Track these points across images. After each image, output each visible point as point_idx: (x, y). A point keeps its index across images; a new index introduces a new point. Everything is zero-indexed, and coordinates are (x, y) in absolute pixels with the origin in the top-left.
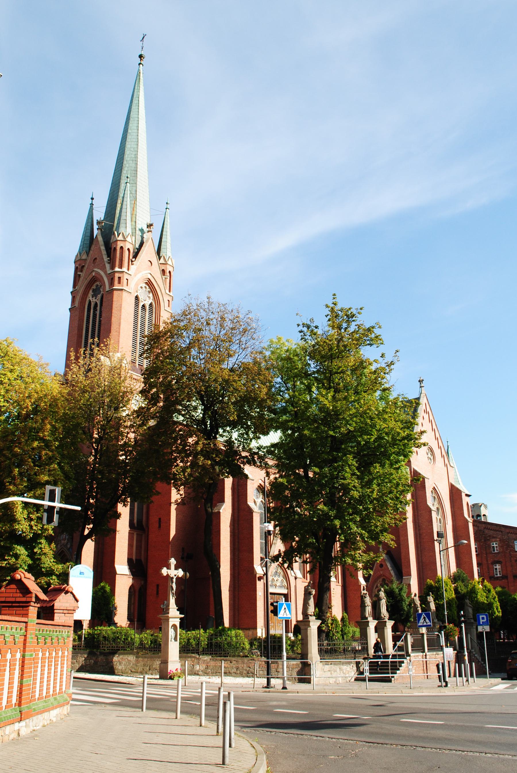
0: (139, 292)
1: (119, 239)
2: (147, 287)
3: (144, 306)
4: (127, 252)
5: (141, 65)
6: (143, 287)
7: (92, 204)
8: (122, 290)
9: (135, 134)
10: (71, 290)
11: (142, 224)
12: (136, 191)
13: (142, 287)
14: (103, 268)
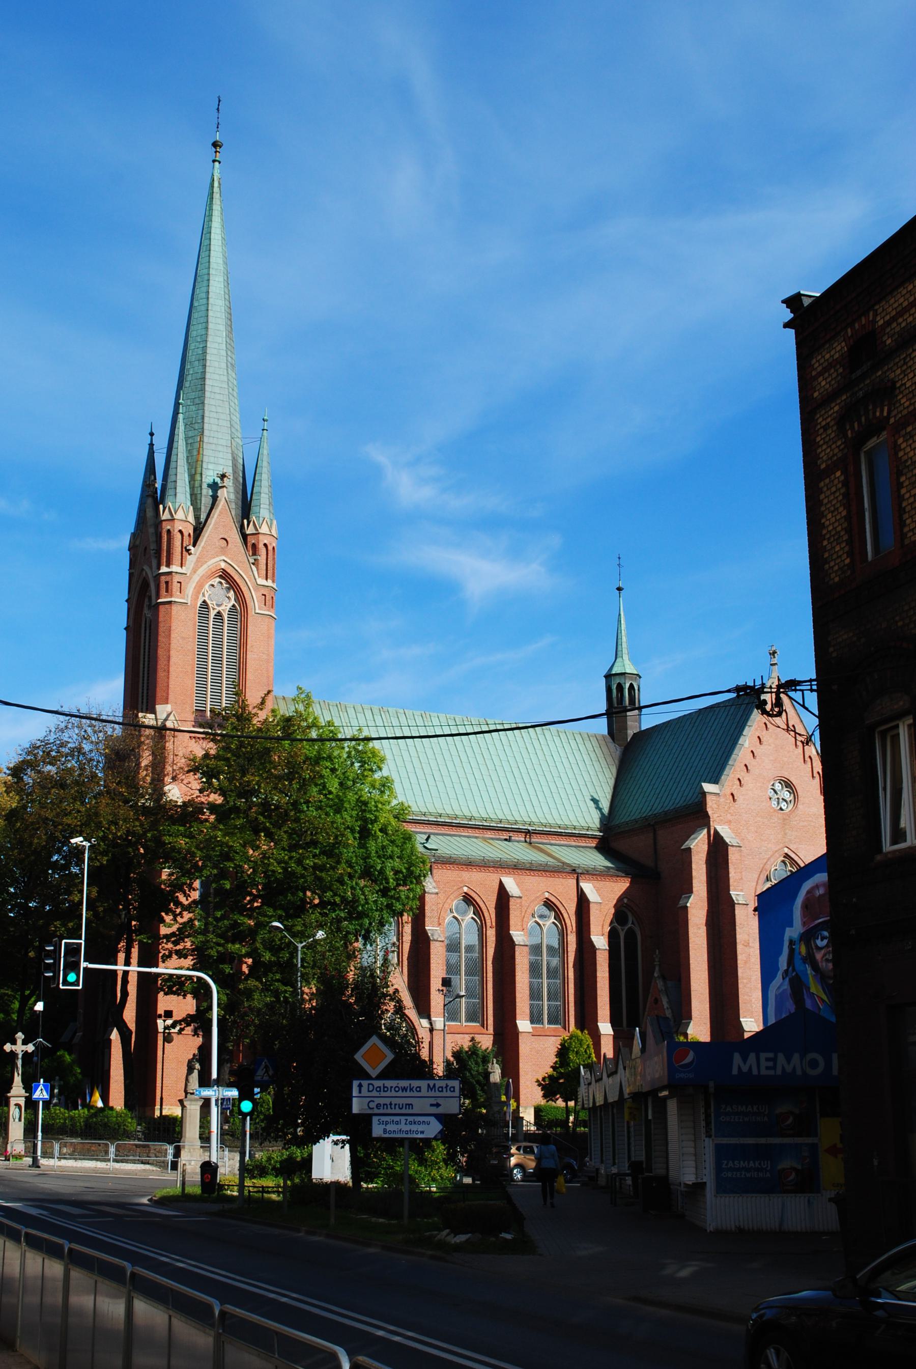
0: (207, 595)
1: (163, 518)
2: (223, 581)
3: (219, 614)
4: (179, 536)
5: (217, 164)
6: (215, 584)
7: (151, 445)
8: (170, 603)
9: (203, 308)
10: (126, 597)
11: (210, 475)
12: (203, 417)
13: (213, 586)
14: (151, 567)
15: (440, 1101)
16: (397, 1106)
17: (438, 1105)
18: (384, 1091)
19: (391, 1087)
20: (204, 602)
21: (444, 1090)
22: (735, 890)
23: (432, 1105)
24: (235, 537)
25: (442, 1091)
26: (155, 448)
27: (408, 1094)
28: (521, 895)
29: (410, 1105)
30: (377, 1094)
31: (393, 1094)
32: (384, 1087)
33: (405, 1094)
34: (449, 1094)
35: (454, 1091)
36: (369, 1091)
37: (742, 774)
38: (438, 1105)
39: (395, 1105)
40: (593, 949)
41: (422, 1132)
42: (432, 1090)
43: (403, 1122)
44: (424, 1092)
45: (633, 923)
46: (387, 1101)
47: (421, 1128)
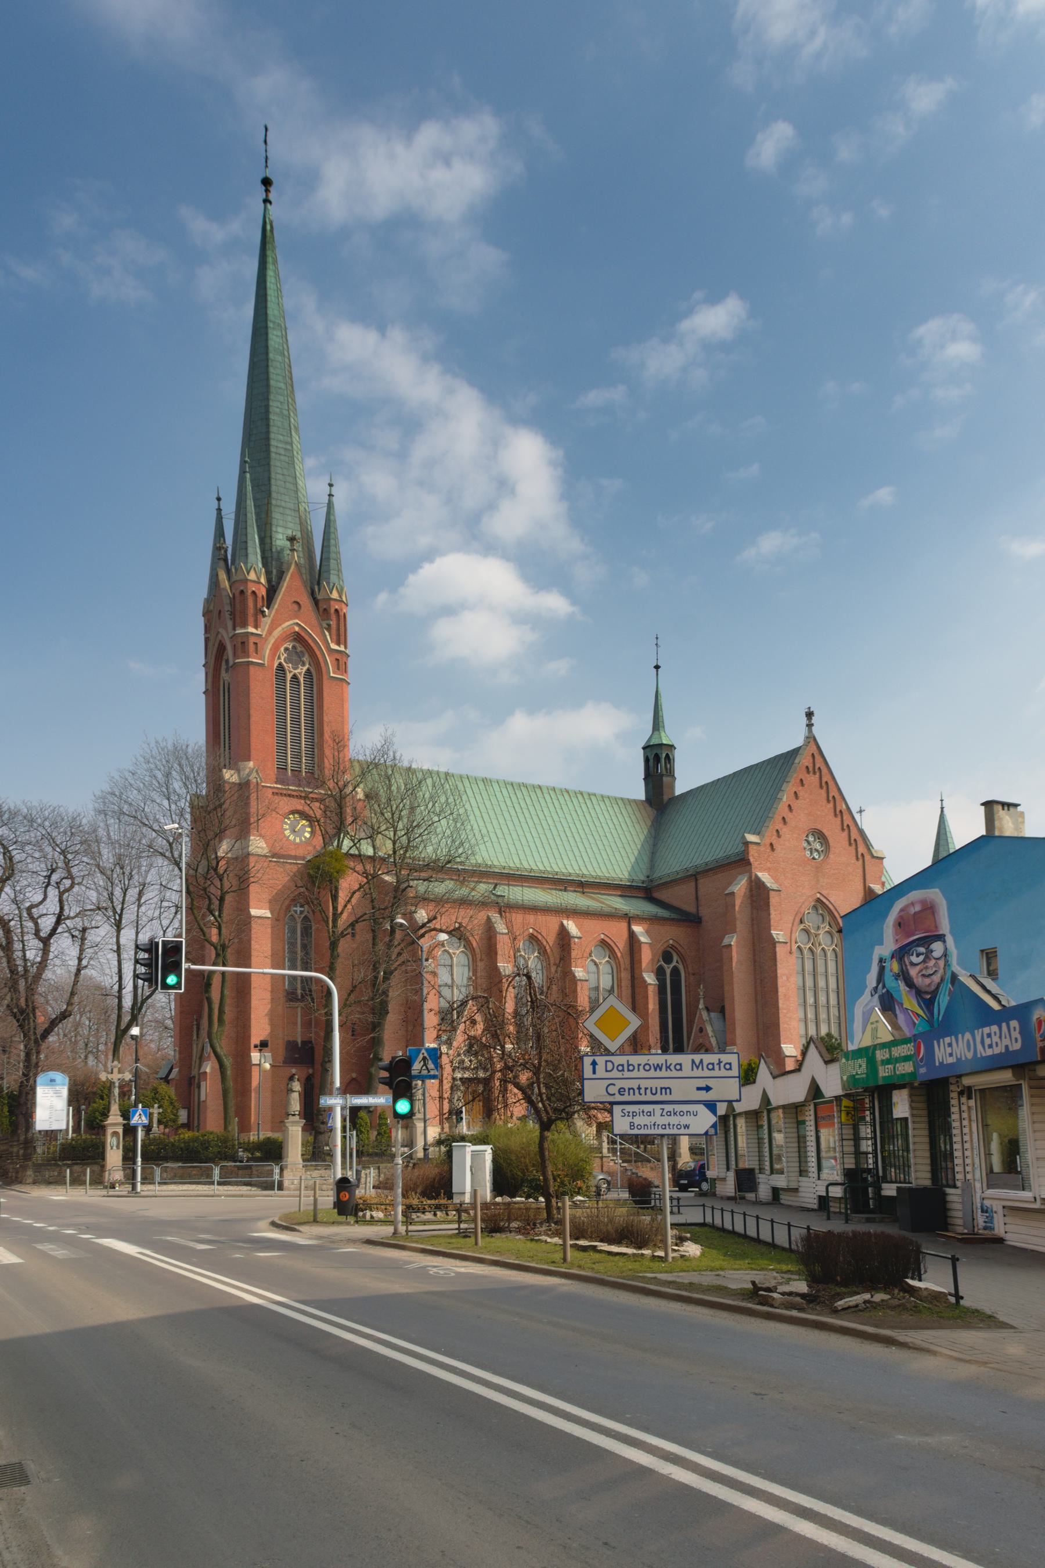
7: (219, 510)
14: (226, 629)
15: (710, 1083)
16: (648, 1091)
17: (708, 1089)
18: (629, 1070)
19: (639, 1065)
20: (280, 664)
21: (716, 1067)
23: (699, 1089)
24: (306, 601)
25: (713, 1069)
26: (223, 513)
27: (664, 1073)
29: (666, 1089)
30: (619, 1075)
31: (642, 1073)
32: (629, 1065)
33: (658, 1074)
34: (724, 1073)
35: (730, 1069)
36: (607, 1071)
37: (779, 825)
38: (708, 1089)
39: (646, 1089)
40: (645, 985)
41: (687, 1127)
42: (698, 1068)
43: (658, 1112)
44: (687, 1070)
45: (677, 962)
46: (634, 1084)
47: (685, 1120)
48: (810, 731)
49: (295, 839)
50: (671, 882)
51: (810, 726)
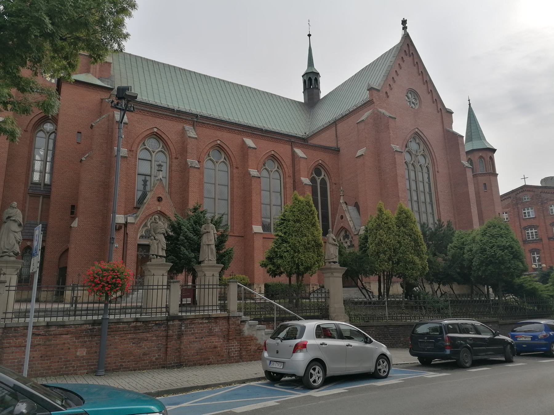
22: (393, 144)
28: (256, 147)
45: (324, 176)
48: (405, 31)
49: (51, 80)
50: (319, 131)
51: (405, 28)
